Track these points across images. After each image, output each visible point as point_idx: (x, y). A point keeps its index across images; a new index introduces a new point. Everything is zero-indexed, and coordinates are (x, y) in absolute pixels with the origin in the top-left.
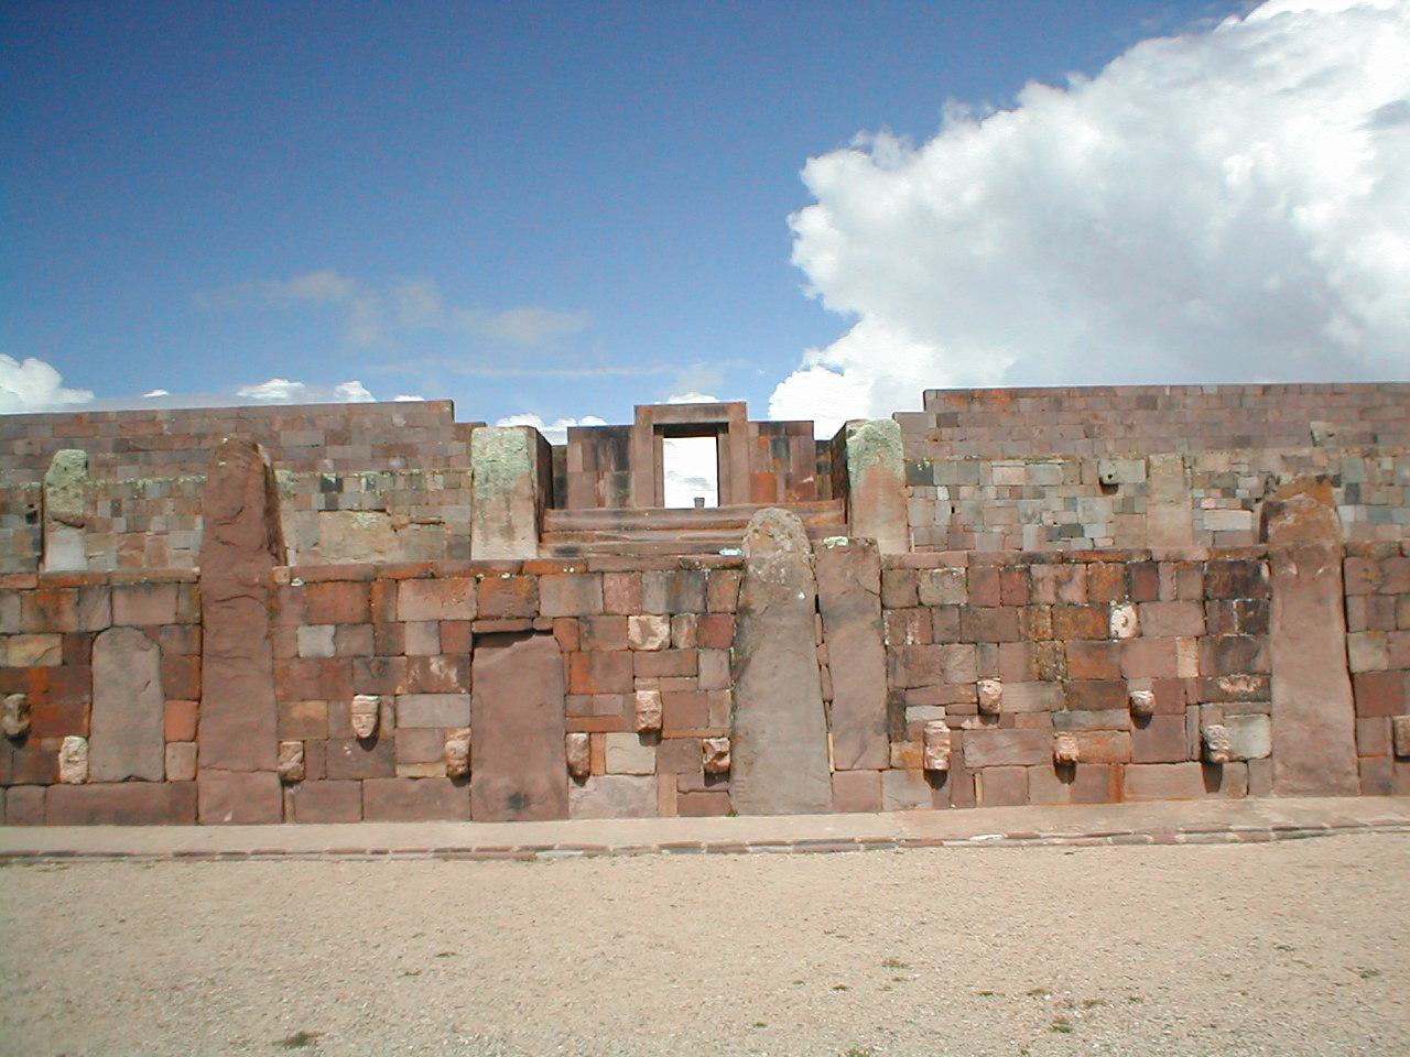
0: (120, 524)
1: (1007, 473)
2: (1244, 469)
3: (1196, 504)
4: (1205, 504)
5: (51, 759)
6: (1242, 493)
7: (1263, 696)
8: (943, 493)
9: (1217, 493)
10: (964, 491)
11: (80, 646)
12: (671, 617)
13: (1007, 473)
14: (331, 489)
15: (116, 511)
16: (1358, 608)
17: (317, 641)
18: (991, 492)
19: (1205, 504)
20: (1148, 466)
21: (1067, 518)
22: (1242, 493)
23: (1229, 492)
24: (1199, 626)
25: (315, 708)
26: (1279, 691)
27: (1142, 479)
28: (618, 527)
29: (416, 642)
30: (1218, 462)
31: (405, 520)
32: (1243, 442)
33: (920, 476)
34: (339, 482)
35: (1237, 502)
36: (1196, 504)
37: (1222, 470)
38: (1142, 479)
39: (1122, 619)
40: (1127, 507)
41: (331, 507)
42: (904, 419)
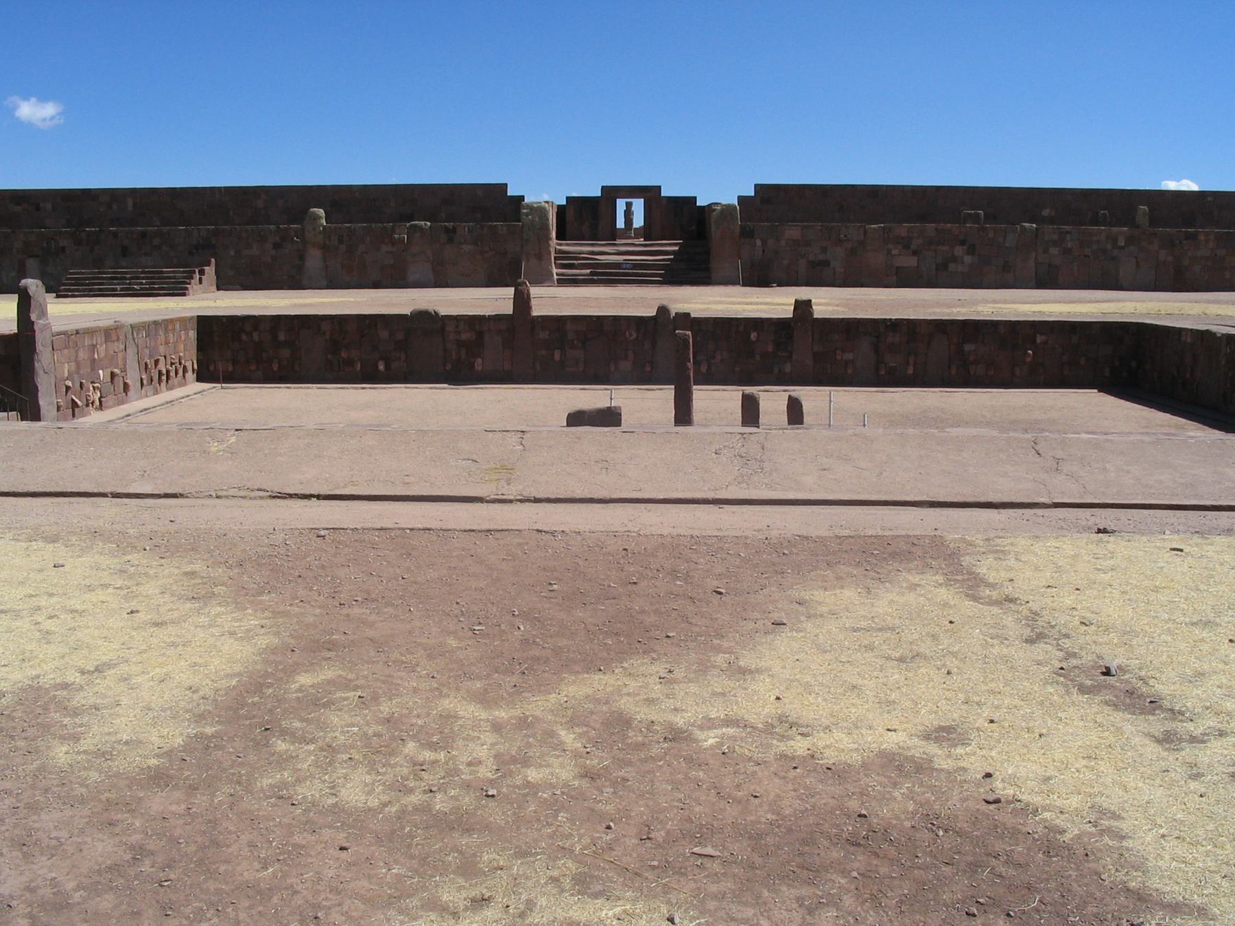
0: (343, 248)
3: (889, 252)
4: (894, 252)
5: (472, 366)
6: (913, 247)
8: (759, 243)
10: (770, 242)
11: (480, 335)
13: (792, 232)
14: (451, 232)
15: (341, 241)
17: (544, 335)
18: (783, 243)
19: (894, 252)
20: (865, 232)
21: (821, 257)
22: (913, 247)
23: (907, 247)
25: (544, 352)
26: (794, 357)
27: (862, 238)
28: (593, 253)
29: (571, 336)
30: (902, 229)
31: (487, 249)
32: (924, 218)
33: (747, 233)
34: (454, 230)
37: (904, 233)
38: (862, 238)
39: (753, 336)
41: (450, 241)
42: (742, 199)
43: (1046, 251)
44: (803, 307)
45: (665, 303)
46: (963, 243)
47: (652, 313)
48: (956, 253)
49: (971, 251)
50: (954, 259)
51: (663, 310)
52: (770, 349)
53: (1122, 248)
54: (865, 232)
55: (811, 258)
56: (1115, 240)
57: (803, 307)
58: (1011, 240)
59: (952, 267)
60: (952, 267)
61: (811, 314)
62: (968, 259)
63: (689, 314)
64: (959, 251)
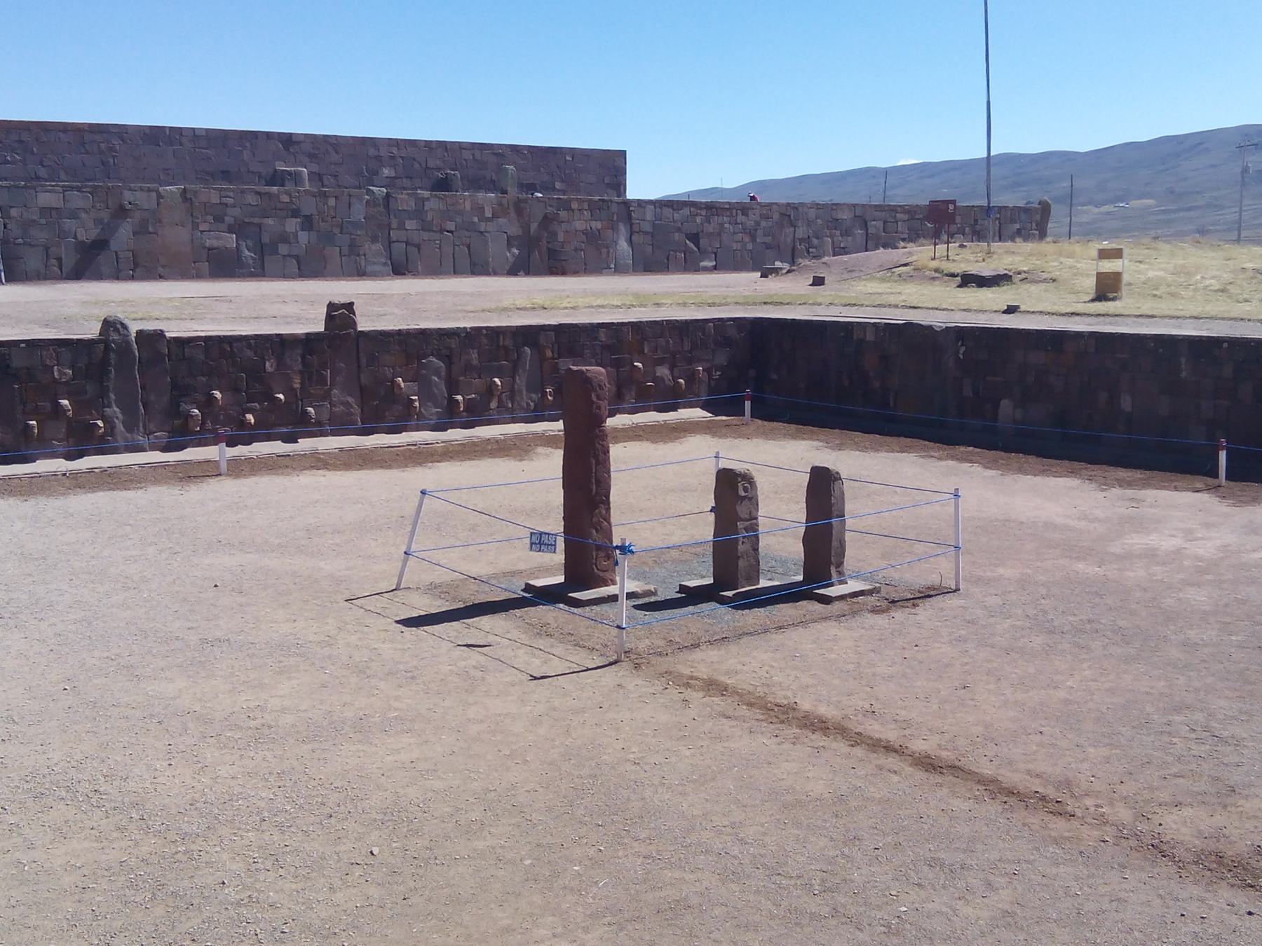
1: (46, 199)
2: (230, 201)
3: (195, 226)
7: (327, 396)
9: (210, 218)
12: (72, 367)
16: (364, 360)
23: (219, 219)
24: (300, 367)
30: (211, 194)
32: (226, 175)
35: (224, 226)
36: (195, 226)
37: (215, 199)
39: (269, 366)
40: (141, 231)
43: (401, 227)
44: (340, 315)
45: (119, 313)
46: (295, 213)
47: (92, 331)
48: (288, 229)
49: (308, 224)
50: (284, 238)
51: (110, 325)
52: (297, 386)
53: (488, 220)
54: (160, 196)
55: (82, 235)
56: (481, 209)
57: (340, 315)
58: (359, 212)
59: (283, 249)
60: (283, 249)
61: (355, 323)
62: (303, 237)
63: (160, 334)
64: (292, 225)
